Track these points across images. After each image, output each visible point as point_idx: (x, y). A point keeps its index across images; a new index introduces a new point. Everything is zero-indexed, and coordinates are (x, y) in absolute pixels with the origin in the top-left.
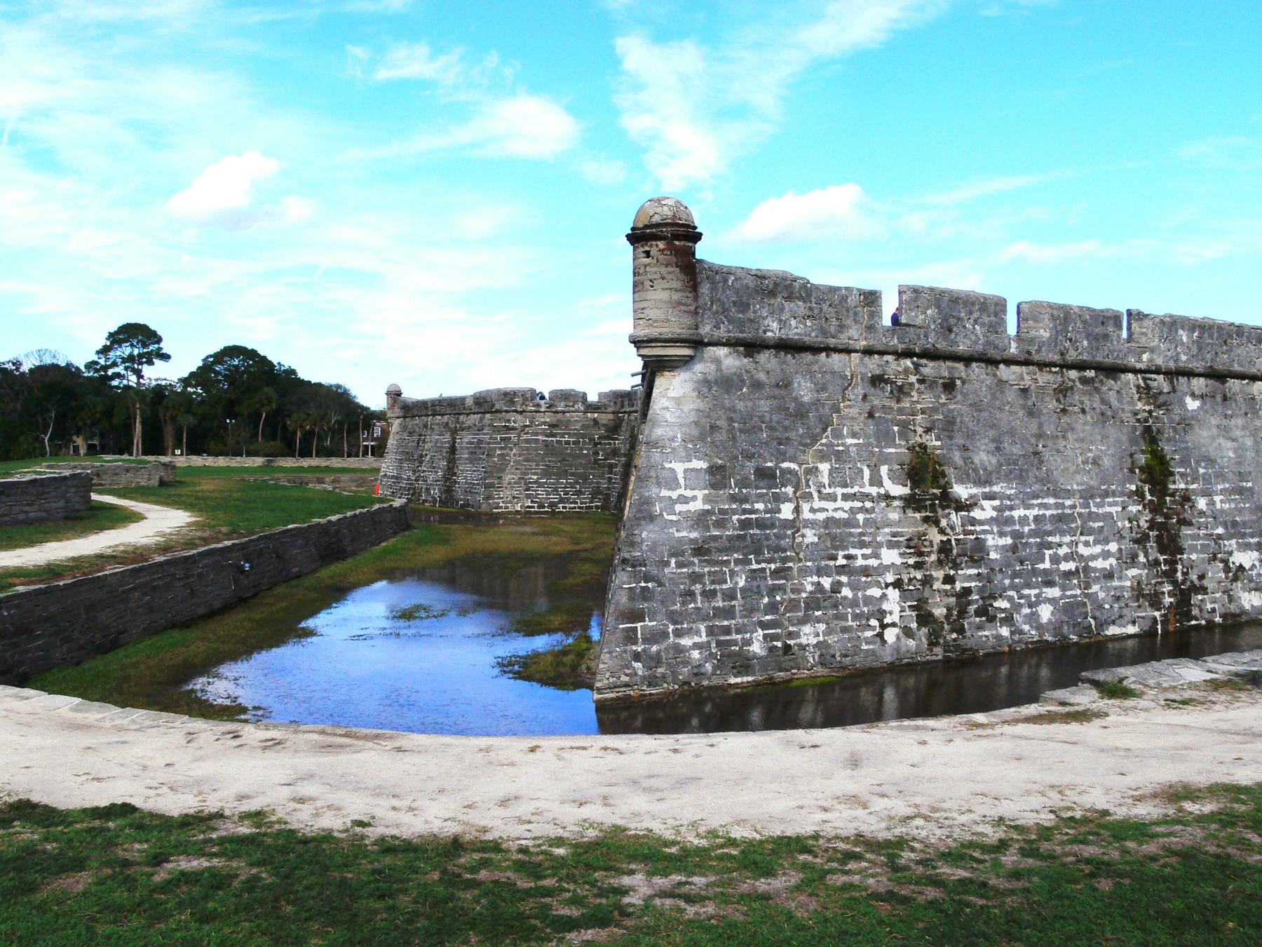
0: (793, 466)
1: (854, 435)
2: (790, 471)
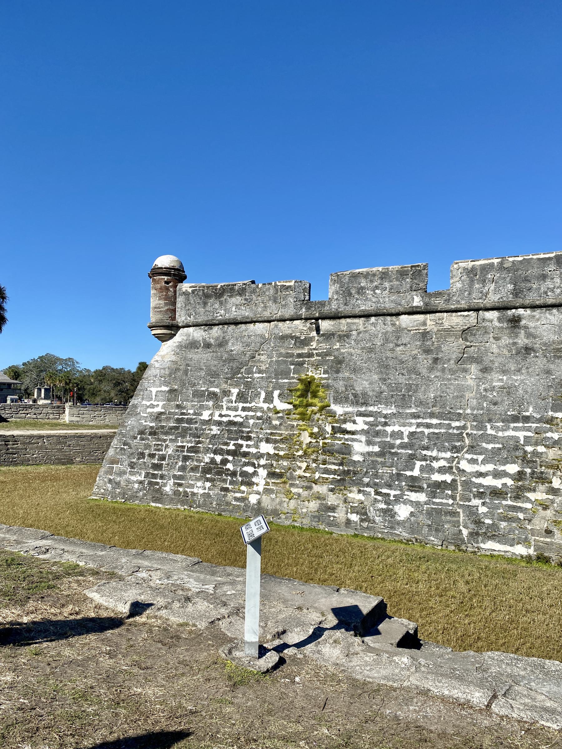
0: (217, 390)
1: (260, 372)
2: (215, 394)
